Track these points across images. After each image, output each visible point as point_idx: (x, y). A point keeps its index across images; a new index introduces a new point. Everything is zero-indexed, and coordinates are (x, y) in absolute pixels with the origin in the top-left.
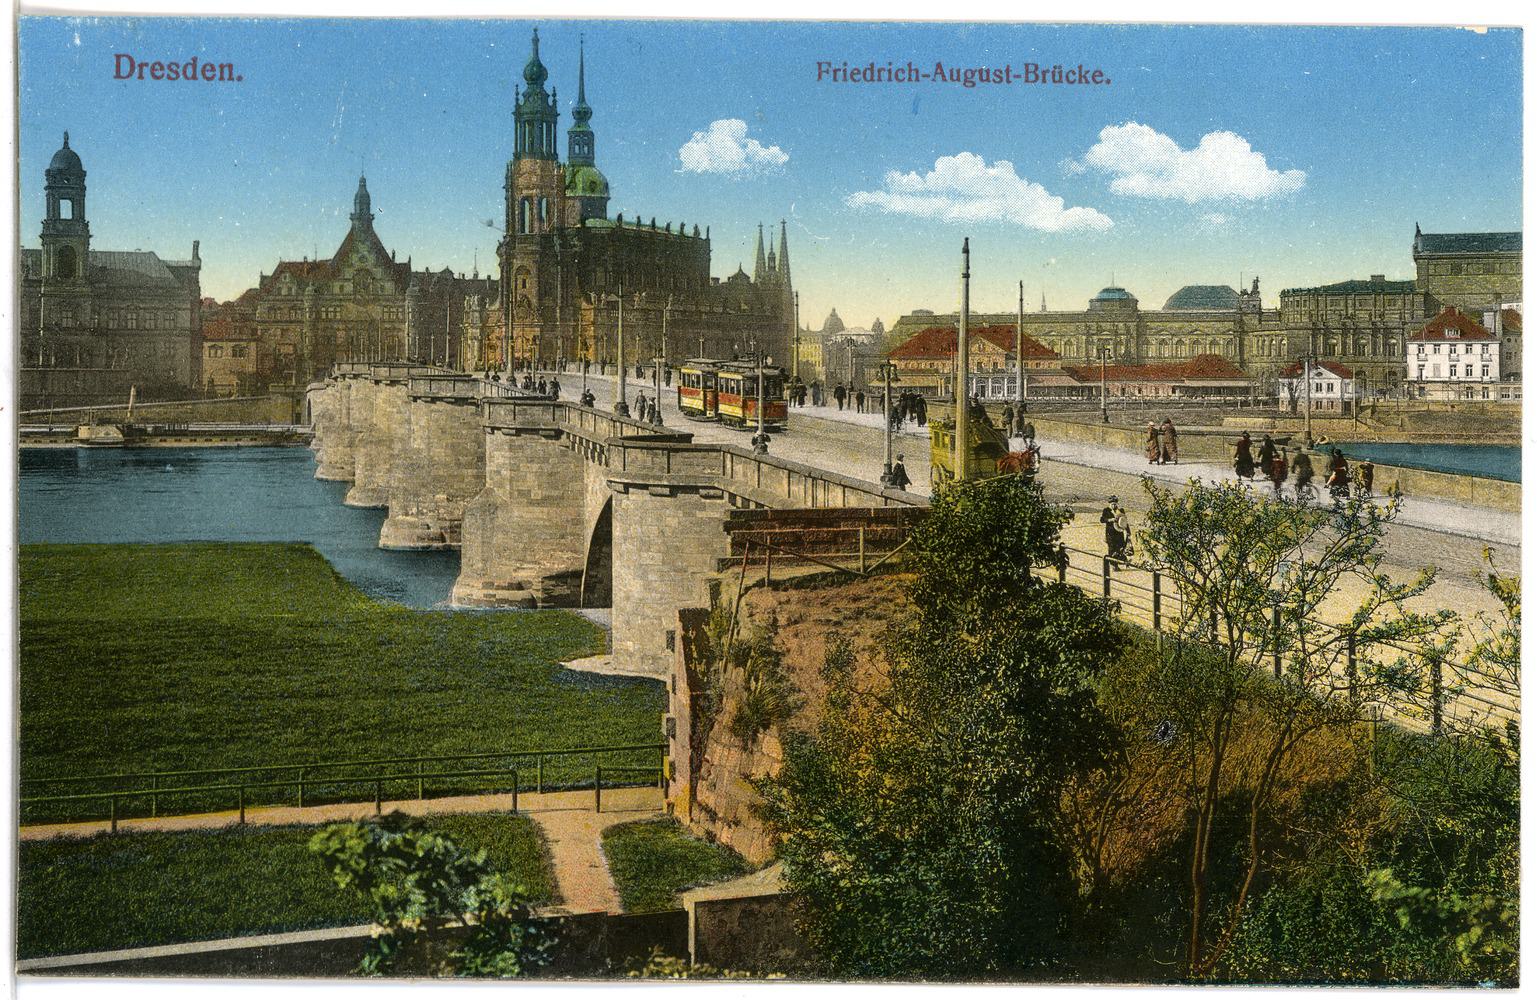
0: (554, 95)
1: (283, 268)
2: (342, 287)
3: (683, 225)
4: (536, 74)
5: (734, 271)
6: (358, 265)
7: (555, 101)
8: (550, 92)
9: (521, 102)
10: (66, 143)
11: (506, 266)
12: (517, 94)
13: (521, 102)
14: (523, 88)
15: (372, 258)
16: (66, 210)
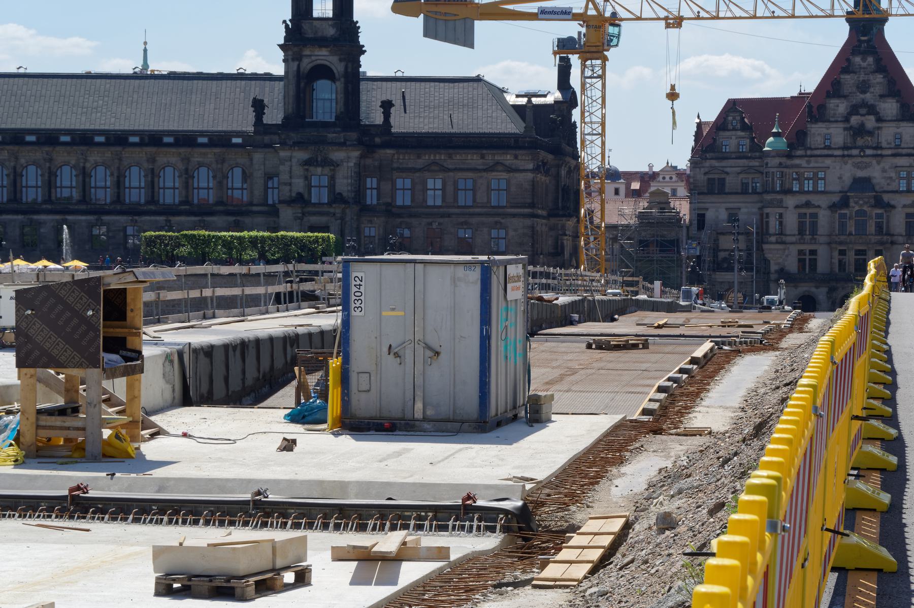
1: (732, 106)
2: (827, 137)
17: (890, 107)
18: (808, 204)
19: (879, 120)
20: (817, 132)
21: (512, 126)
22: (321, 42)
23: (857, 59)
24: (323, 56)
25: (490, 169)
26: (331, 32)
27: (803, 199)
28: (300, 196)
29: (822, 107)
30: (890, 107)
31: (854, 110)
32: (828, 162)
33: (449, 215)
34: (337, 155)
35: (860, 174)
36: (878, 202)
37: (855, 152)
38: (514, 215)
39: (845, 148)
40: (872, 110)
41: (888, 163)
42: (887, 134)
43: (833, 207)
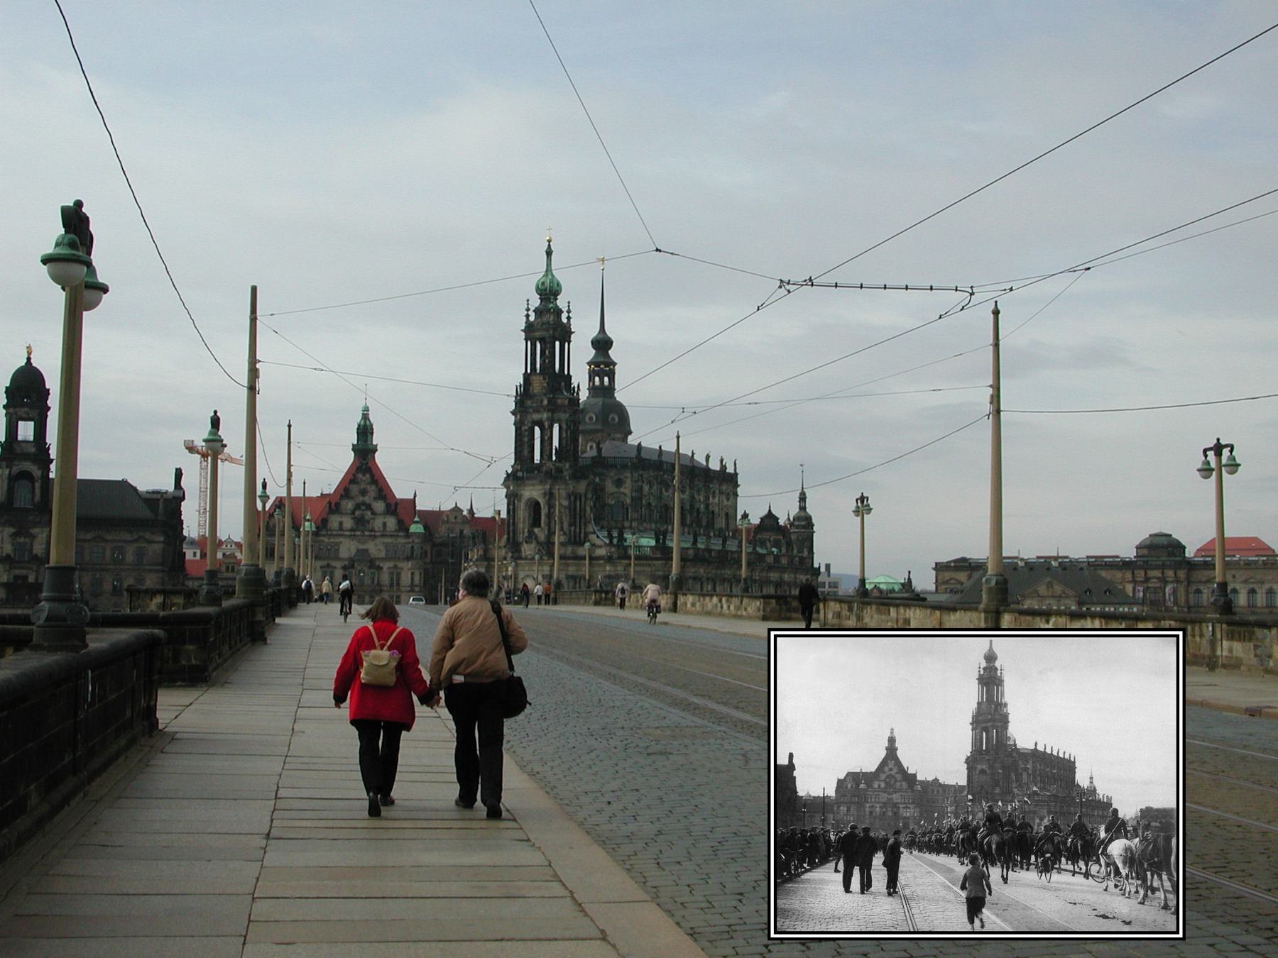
0: (569, 312)
2: (341, 523)
3: (708, 457)
4: (549, 292)
5: (766, 512)
6: (361, 499)
7: (569, 318)
8: (565, 310)
9: (532, 318)
10: (29, 359)
11: (512, 498)
12: (528, 310)
13: (532, 318)
14: (536, 302)
15: (372, 490)
16: (26, 430)
17: (379, 506)
18: (328, 565)
19: (373, 513)
20: (334, 521)
21: (146, 513)
22: (26, 457)
23: (360, 476)
24: (28, 466)
25: (136, 540)
26: (33, 450)
27: (325, 563)
28: (8, 556)
29: (337, 505)
30: (379, 506)
31: (358, 507)
32: (342, 539)
33: (108, 570)
34: (35, 531)
35: (361, 547)
36: (373, 564)
37: (358, 533)
38: (150, 571)
39: (352, 530)
40: (369, 507)
41: (379, 541)
42: (378, 523)
43: (344, 568)
